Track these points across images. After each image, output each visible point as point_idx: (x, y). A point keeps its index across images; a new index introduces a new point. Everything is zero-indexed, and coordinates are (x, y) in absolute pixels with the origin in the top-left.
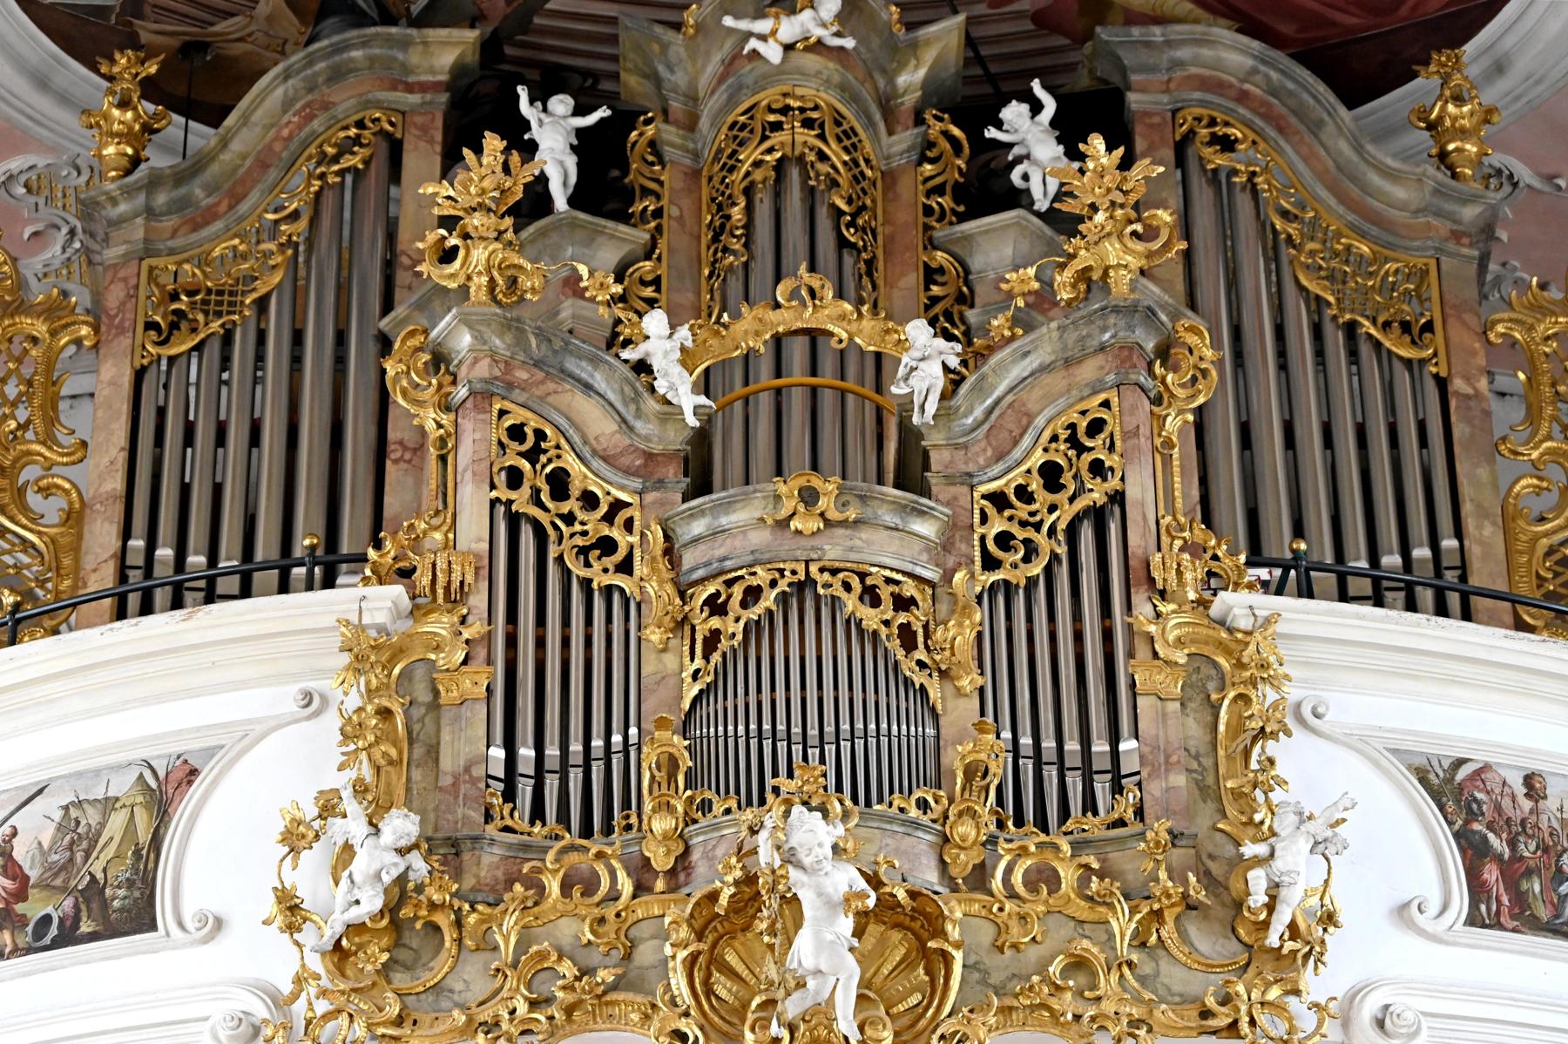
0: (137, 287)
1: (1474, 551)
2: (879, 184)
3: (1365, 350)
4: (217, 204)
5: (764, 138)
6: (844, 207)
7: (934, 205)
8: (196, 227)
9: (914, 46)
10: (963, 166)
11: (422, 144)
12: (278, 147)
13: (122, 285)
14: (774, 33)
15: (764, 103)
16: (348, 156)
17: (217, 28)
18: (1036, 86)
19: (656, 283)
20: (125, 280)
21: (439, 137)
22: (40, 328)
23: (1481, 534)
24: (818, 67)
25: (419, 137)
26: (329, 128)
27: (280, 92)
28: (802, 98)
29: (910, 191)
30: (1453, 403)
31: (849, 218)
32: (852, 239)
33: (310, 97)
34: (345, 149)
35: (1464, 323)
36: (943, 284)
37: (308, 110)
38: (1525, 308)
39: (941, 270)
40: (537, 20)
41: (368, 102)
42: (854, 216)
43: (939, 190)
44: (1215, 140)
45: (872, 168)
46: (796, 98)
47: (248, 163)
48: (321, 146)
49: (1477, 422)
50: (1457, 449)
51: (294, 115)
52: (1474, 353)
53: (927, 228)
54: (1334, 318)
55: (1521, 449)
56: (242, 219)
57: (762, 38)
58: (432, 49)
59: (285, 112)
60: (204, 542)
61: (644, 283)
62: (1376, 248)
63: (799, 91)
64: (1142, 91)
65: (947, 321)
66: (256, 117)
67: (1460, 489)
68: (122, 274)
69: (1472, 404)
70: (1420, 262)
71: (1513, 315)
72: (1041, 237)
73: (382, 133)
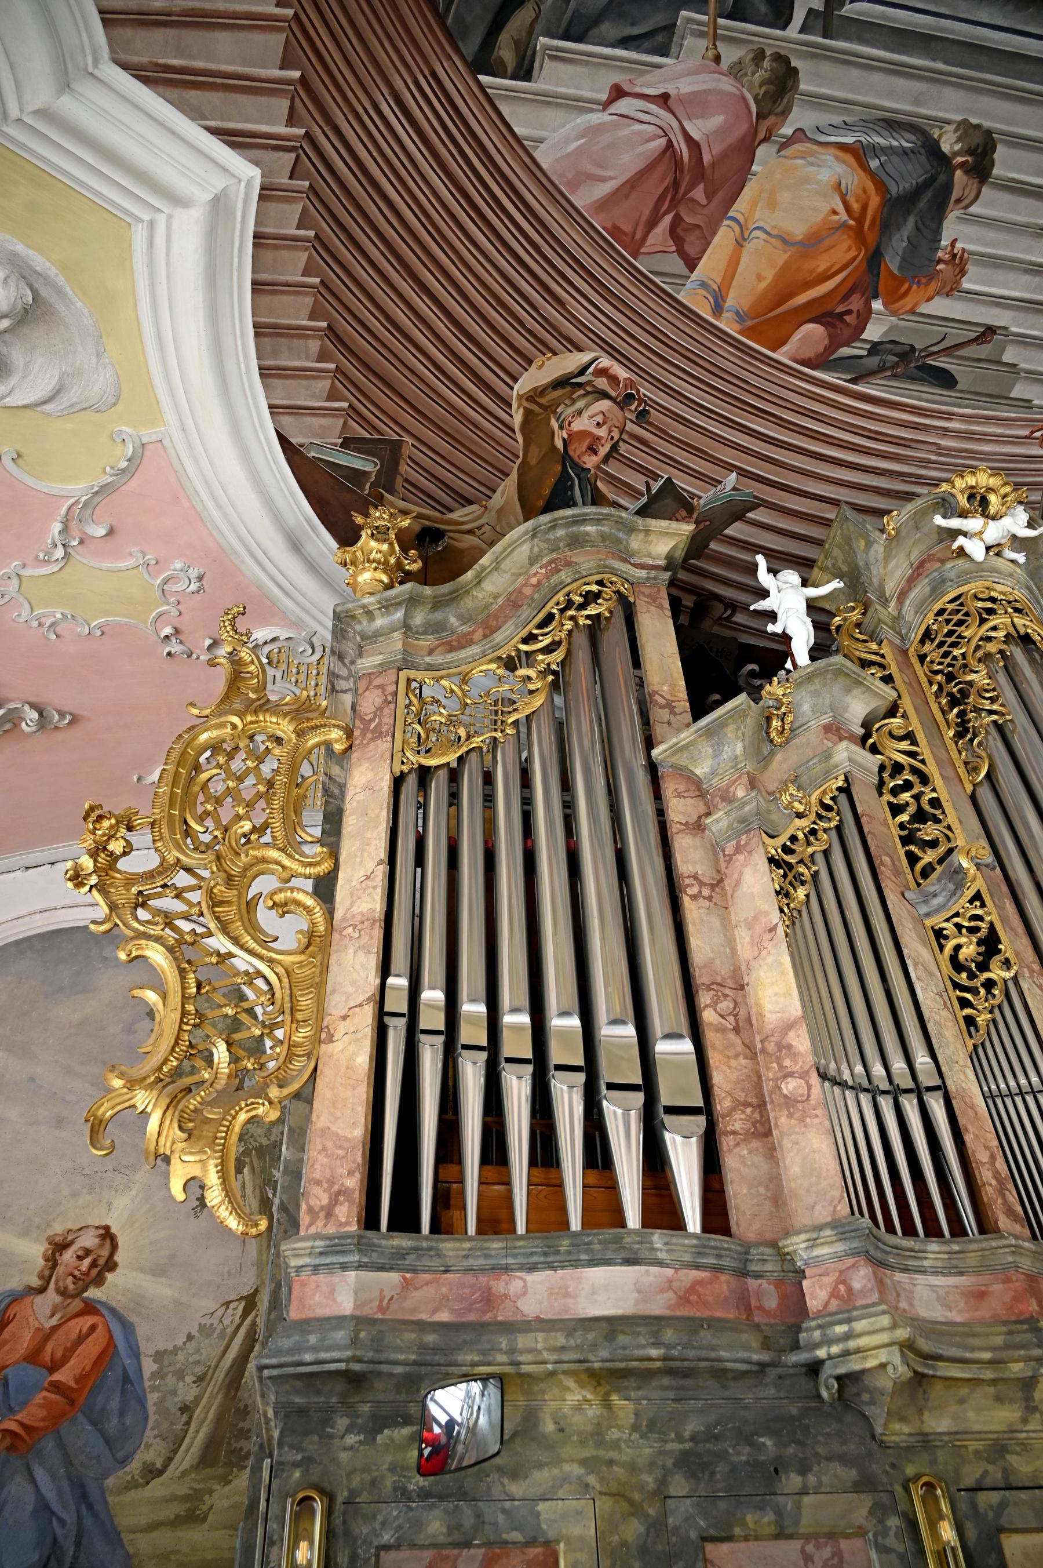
0: (396, 693)
4: (473, 632)
8: (452, 649)
11: (653, 608)
12: (527, 591)
13: (379, 692)
16: (593, 605)
17: (453, 516)
19: (910, 737)
20: (382, 687)
22: (285, 728)
25: (649, 603)
26: (575, 581)
27: (526, 548)
33: (554, 555)
34: (590, 598)
37: (553, 565)
41: (605, 566)
47: (500, 601)
48: (568, 595)
51: (541, 568)
56: (497, 647)
58: (652, 538)
59: (532, 565)
60: (481, 988)
68: (378, 681)
73: (618, 593)
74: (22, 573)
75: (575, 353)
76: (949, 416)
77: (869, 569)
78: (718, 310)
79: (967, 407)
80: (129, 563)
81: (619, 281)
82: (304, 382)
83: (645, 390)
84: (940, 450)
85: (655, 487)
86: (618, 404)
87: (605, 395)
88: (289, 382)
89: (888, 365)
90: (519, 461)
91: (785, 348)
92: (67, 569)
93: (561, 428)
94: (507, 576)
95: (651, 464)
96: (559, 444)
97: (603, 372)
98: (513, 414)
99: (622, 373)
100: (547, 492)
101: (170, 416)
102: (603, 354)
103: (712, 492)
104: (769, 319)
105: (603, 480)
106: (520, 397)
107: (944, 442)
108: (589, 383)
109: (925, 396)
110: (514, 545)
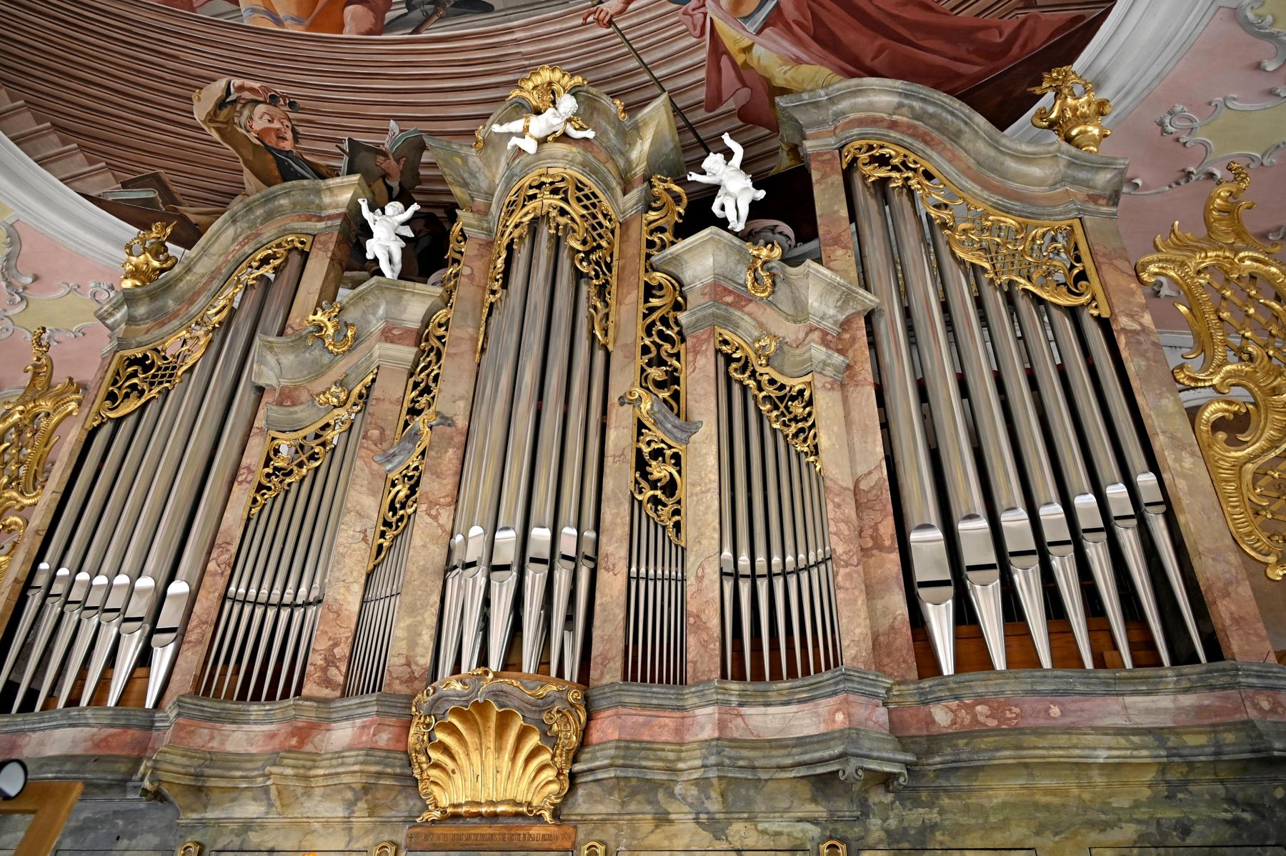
1: (1179, 487)
2: (617, 232)
3: (1023, 304)
5: (524, 206)
6: (580, 248)
7: (656, 240)
9: (637, 128)
10: (682, 211)
14: (526, 129)
15: (527, 184)
18: (726, 137)
21: (332, 247)
23: (1181, 466)
24: (565, 152)
25: (320, 249)
28: (553, 176)
29: (639, 233)
30: (1122, 341)
31: (582, 255)
32: (585, 271)
35: (1116, 268)
36: (660, 297)
38: (1172, 248)
39: (660, 287)
40: (422, 172)
41: (285, 230)
42: (588, 253)
43: (661, 230)
44: (873, 159)
45: (610, 220)
46: (547, 175)
49: (1150, 355)
50: (1135, 384)
52: (1133, 293)
53: (648, 256)
54: (992, 281)
55: (1201, 376)
57: (521, 135)
61: (440, 325)
62: (1021, 219)
63: (551, 171)
64: (813, 139)
65: (663, 325)
66: (215, 249)
67: (1147, 422)
69: (1141, 338)
70: (1064, 224)
71: (1160, 256)
72: (732, 246)
74: (7, 314)
75: (213, 83)
76: (510, 30)
77: (475, 177)
78: (278, 22)
79: (517, 19)
80: (62, 292)
81: (199, 30)
82: (67, 160)
83: (280, 90)
84: (525, 56)
85: (346, 146)
86: (270, 104)
87: (258, 102)
88: (59, 163)
89: (430, 13)
90: (241, 160)
91: (347, 29)
92: (30, 304)
93: (248, 131)
94: (215, 258)
95: (330, 134)
96: (258, 142)
97: (241, 88)
98: (209, 132)
99: (256, 85)
100: (277, 173)
101: (11, 206)
102: (230, 78)
103: (388, 138)
104: (317, 15)
105: (306, 154)
106: (204, 122)
107: (523, 50)
108: (239, 98)
109: (477, 23)
110: (218, 234)
